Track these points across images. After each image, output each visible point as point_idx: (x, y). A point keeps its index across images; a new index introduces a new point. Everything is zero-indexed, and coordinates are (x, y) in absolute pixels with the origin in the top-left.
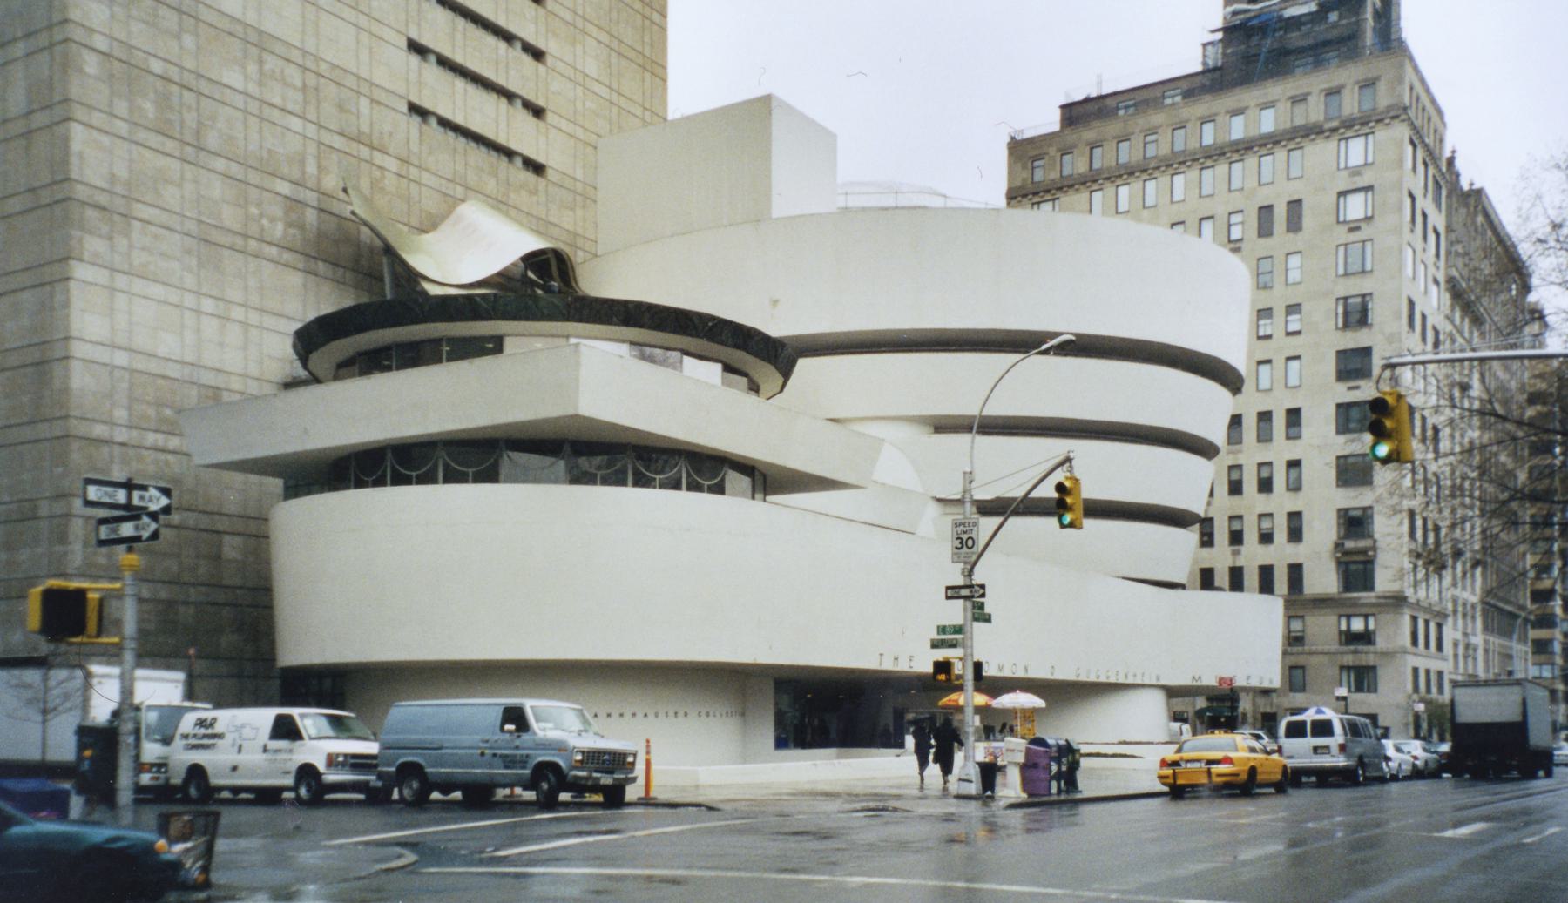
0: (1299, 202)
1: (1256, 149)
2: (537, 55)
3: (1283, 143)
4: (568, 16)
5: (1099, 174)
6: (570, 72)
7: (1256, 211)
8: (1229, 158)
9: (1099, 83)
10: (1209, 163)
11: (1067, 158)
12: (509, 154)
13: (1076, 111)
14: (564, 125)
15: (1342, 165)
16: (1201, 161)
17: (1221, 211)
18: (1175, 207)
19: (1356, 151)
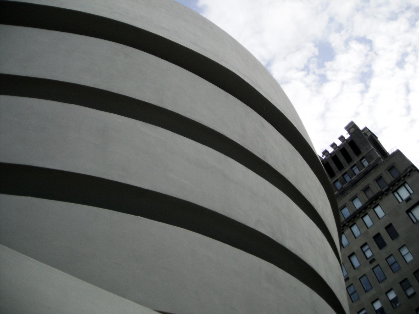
0: (390, 225)
1: (358, 215)
3: (369, 207)
7: (373, 240)
15: (400, 201)
17: (356, 248)
19: (404, 193)
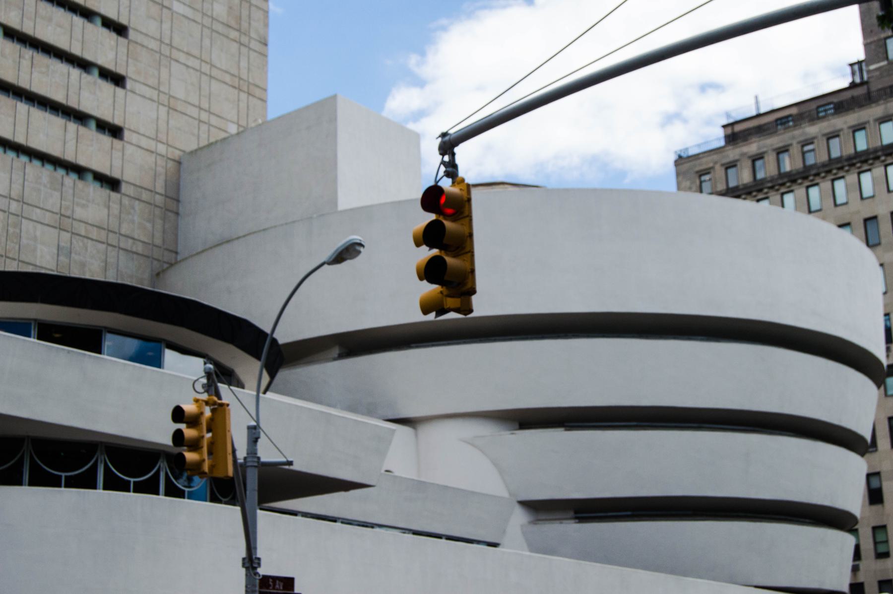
2: (118, 80)
4: (153, 45)
5: (762, 184)
6: (154, 94)
8: (883, 161)
9: (757, 102)
10: (865, 167)
11: (731, 172)
12: (79, 171)
13: (738, 128)
14: (144, 143)
16: (858, 165)
18: (839, 209)
